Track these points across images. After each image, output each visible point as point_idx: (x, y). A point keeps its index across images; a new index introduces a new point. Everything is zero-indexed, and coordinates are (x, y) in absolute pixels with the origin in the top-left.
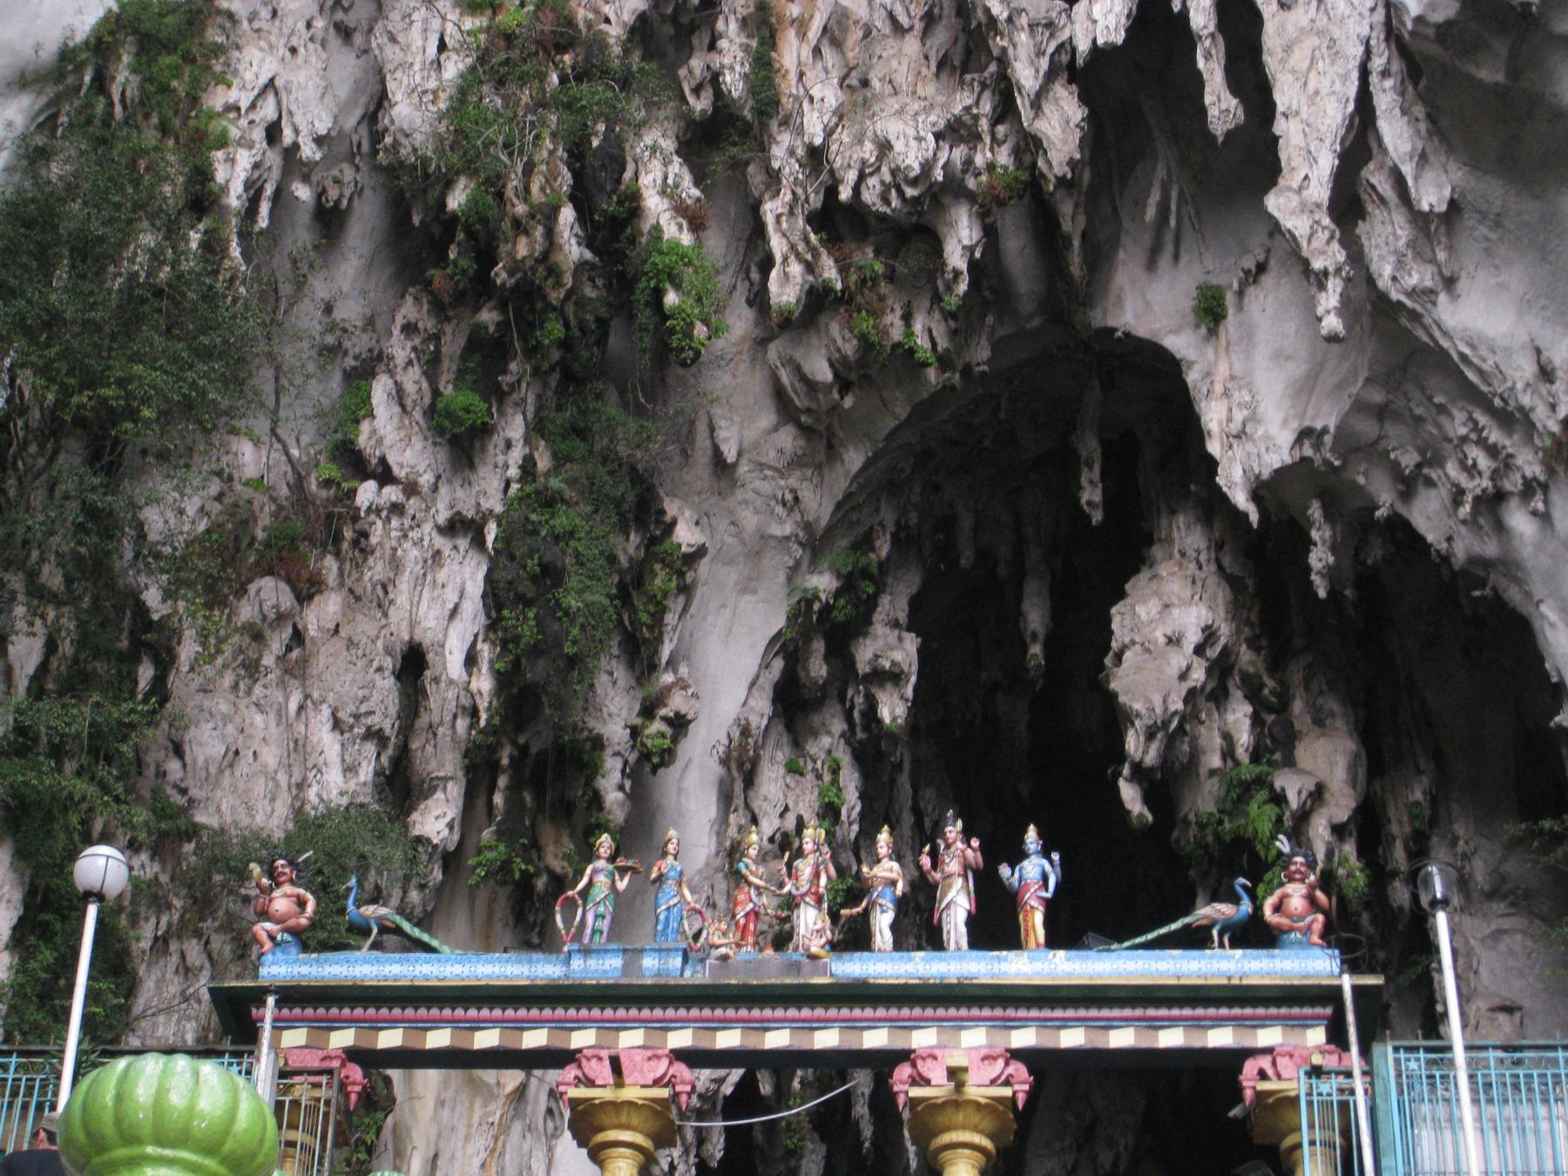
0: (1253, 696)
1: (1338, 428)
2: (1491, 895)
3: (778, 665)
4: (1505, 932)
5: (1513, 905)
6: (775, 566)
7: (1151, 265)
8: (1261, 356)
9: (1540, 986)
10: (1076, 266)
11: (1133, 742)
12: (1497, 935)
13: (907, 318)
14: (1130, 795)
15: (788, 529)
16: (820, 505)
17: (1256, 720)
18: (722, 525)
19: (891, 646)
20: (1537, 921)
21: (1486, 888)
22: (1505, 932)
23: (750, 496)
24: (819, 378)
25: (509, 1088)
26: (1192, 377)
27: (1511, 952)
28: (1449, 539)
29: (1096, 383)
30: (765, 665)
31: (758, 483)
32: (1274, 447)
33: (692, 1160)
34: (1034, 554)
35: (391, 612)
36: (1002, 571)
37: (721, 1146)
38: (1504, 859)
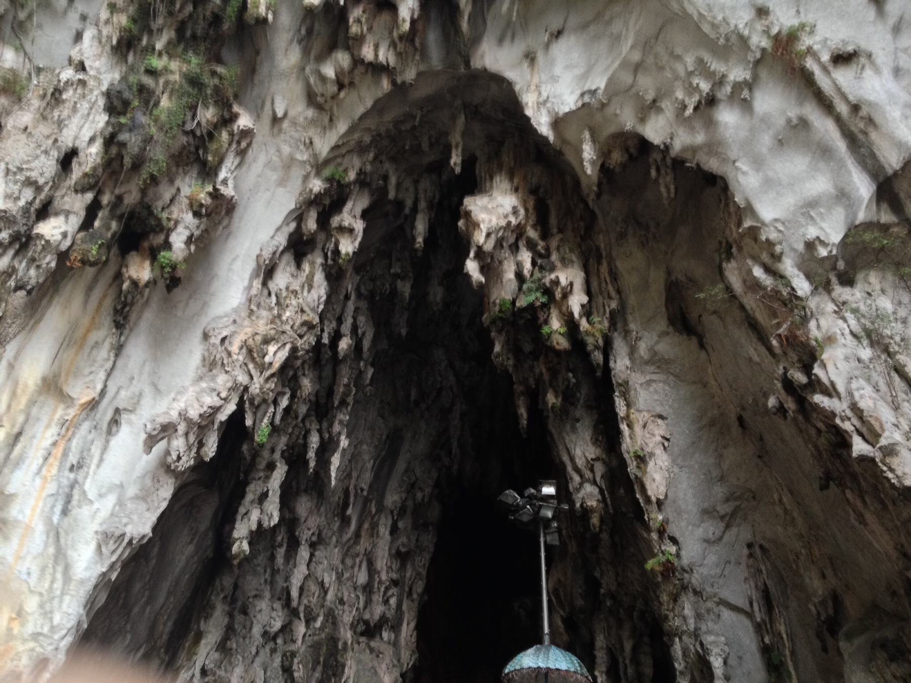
0: (531, 245)
1: (607, 86)
2: (647, 363)
3: (293, 226)
4: (654, 381)
5: (659, 367)
6: (297, 173)
7: (501, 41)
8: (558, 70)
9: (671, 411)
10: (465, 25)
11: (479, 238)
12: (649, 383)
13: (376, 47)
14: (472, 267)
15: (305, 157)
16: (324, 146)
17: (534, 263)
18: (272, 151)
19: (351, 217)
20: (671, 377)
21: (646, 357)
22: (654, 381)
23: (288, 138)
24: (329, 76)
25: (85, 399)
26: (517, 88)
27: (656, 392)
28: (672, 138)
29: (463, 116)
30: (286, 222)
31: (293, 133)
32: (568, 101)
33: (193, 454)
34: (422, 205)
35: (65, 131)
36: (407, 211)
37: (214, 448)
38: (657, 342)
